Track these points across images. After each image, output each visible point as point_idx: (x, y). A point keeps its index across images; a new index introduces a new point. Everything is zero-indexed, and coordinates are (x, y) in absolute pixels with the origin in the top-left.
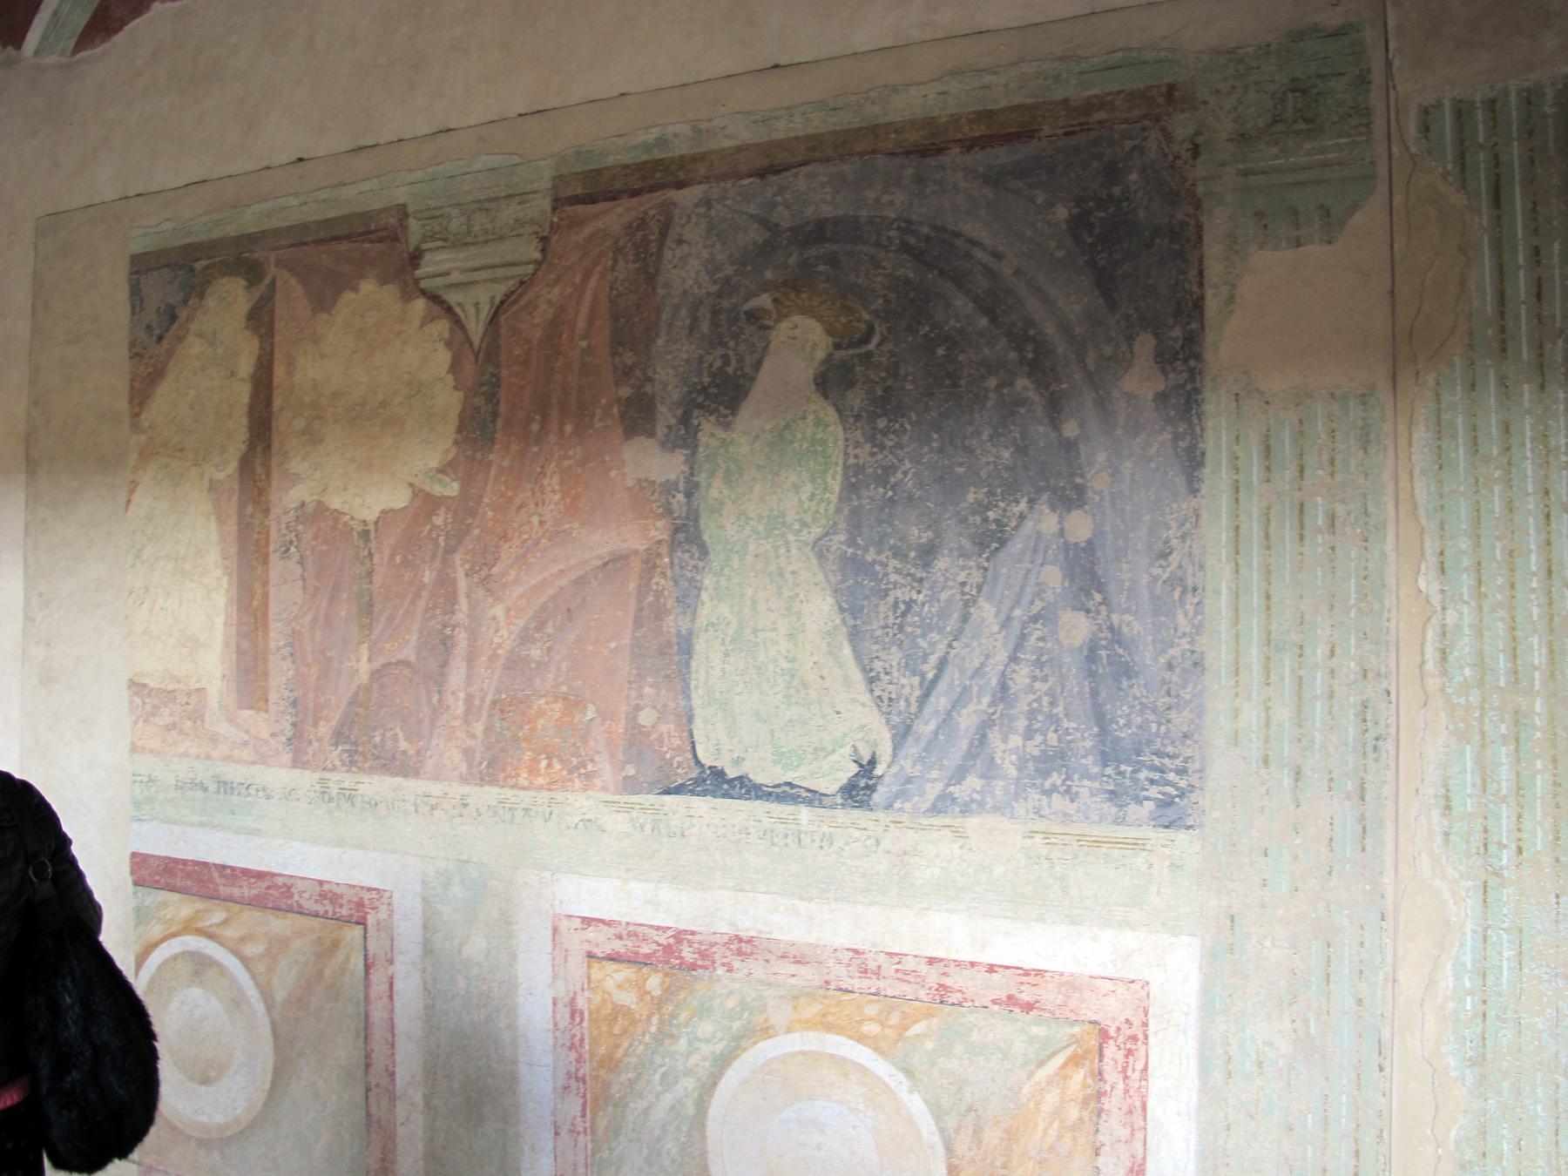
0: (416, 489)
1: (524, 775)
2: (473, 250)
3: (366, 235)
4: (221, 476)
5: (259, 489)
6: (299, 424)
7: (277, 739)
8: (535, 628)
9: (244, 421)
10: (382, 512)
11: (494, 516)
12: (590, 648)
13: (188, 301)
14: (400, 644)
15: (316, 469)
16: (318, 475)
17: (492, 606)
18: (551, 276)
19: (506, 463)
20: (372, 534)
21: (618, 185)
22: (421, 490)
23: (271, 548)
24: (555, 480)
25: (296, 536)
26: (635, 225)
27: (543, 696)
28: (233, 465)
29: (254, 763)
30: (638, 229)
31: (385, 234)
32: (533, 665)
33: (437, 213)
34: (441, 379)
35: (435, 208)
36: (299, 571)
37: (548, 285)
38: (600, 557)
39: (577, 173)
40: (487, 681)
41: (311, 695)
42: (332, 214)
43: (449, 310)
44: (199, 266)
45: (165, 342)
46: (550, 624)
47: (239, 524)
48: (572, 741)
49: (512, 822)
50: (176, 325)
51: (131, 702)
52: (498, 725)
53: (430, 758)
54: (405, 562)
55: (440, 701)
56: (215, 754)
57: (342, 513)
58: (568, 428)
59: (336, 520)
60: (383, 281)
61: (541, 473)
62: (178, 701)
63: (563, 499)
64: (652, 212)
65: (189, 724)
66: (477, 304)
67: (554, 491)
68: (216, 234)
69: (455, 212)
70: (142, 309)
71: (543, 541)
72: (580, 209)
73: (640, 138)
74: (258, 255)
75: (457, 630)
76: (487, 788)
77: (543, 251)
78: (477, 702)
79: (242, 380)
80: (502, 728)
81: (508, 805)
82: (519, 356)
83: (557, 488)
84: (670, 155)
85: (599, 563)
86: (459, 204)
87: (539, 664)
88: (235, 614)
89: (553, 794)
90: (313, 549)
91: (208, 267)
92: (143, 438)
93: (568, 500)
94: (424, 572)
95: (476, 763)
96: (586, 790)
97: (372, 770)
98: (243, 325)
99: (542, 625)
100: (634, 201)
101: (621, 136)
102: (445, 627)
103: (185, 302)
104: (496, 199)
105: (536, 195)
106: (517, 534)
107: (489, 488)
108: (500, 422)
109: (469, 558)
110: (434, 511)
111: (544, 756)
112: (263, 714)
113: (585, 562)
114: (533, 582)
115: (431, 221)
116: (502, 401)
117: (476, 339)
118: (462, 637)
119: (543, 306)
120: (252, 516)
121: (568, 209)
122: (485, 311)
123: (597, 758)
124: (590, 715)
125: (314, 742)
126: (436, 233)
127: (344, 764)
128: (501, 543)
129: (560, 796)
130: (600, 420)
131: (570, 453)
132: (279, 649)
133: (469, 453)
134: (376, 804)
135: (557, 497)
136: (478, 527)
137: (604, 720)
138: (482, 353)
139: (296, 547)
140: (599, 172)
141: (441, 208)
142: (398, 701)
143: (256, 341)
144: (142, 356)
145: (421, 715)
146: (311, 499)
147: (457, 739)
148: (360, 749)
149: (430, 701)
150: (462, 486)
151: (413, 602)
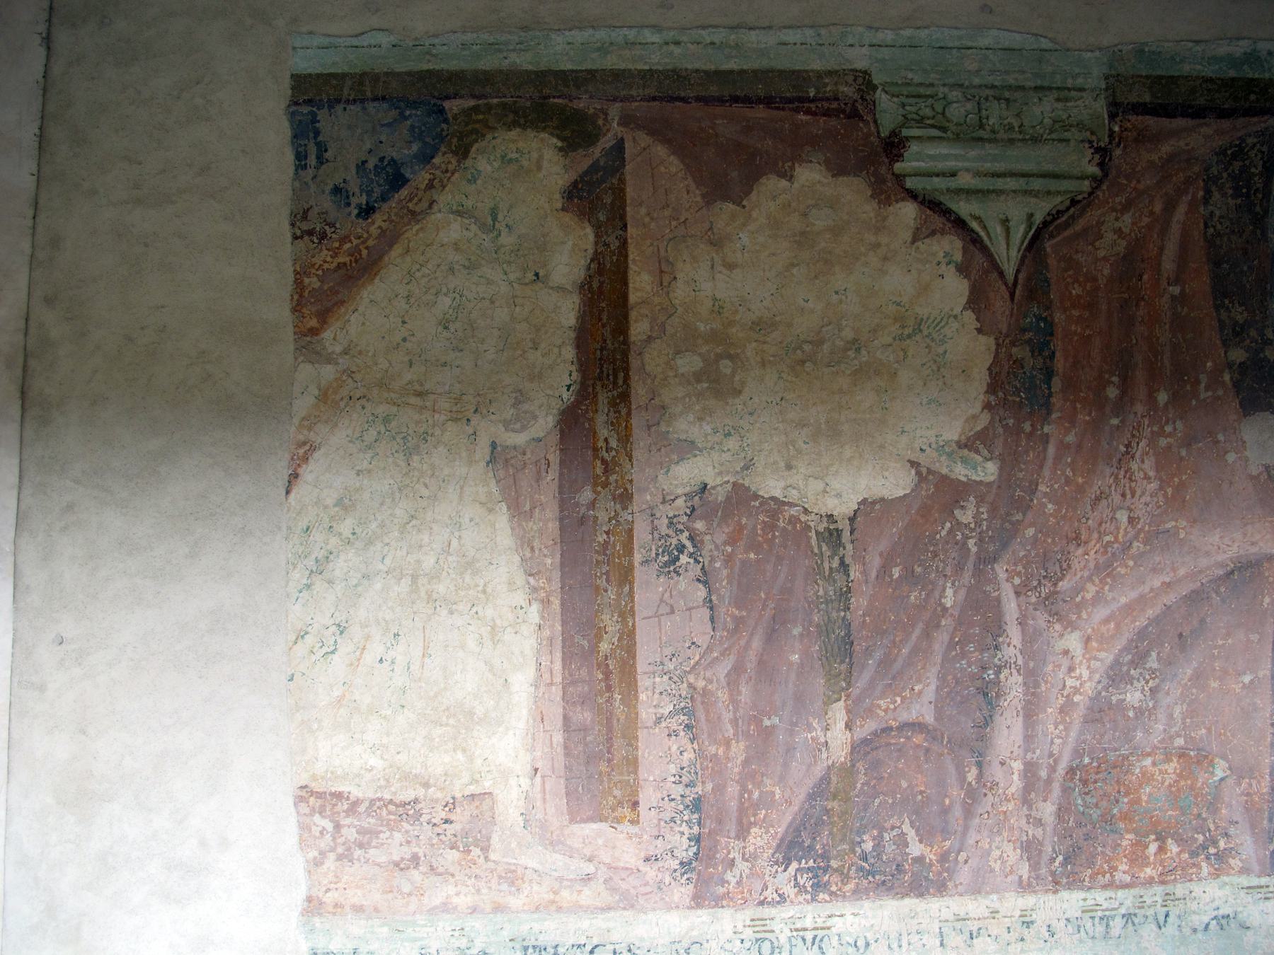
0: (924, 471)
1: (1123, 867)
2: (991, 149)
3: (800, 102)
4: (520, 439)
5: (604, 461)
6: (689, 363)
7: (660, 864)
8: (1132, 662)
9: (569, 353)
10: (865, 500)
11: (1059, 510)
12: (1214, 684)
13: (432, 157)
14: (903, 699)
15: (728, 435)
16: (732, 443)
17: (1061, 636)
18: (1118, 200)
19: (1070, 438)
20: (846, 535)
21: (1201, 101)
22: (929, 471)
23: (638, 558)
24: (1149, 464)
25: (691, 538)
26: (1229, 152)
27: (1149, 755)
28: (545, 423)
29: (609, 908)
30: (1234, 157)
31: (835, 105)
32: (1131, 714)
33: (922, 90)
34: (955, 317)
35: (921, 84)
36: (701, 592)
37: (1113, 209)
38: (1221, 565)
39: (1141, 76)
40: (1057, 741)
41: (733, 789)
42: (732, 65)
43: (960, 224)
44: (453, 106)
45: (379, 220)
46: (1154, 654)
47: (561, 520)
48: (1195, 811)
49: (1106, 936)
50: (404, 192)
51: (304, 828)
52: (1079, 801)
53: (966, 862)
54: (909, 574)
55: (980, 776)
56: (515, 902)
57: (784, 503)
58: (1162, 397)
59: (774, 515)
60: (838, 170)
61: (1127, 453)
62: (424, 818)
63: (1161, 488)
64: (1250, 141)
65: (453, 855)
66: (1005, 222)
67: (1147, 477)
68: (488, 63)
69: (955, 94)
70: (321, 160)
71: (1135, 544)
72: (1150, 121)
73: (1223, 50)
74: (583, 103)
75: (1005, 672)
76: (1064, 894)
77: (1101, 165)
78: (1043, 774)
79: (560, 289)
80: (1085, 805)
81: (1100, 914)
82: (1078, 296)
83: (1152, 474)
84: (1267, 76)
85: (1221, 572)
86: (961, 86)
87: (1139, 712)
88: (558, 666)
89: (1169, 888)
90: (729, 559)
91: (475, 109)
92: (328, 372)
93: (1170, 491)
94: (944, 590)
95: (1045, 858)
96: (1218, 876)
97: (858, 893)
98: (559, 205)
99: (1139, 659)
100: (1226, 124)
101: (1197, 42)
102: (984, 668)
103: (426, 158)
104: (1022, 88)
105: (1084, 94)
106: (1095, 535)
107: (1046, 472)
108: (1057, 383)
109: (1020, 568)
110: (957, 502)
111: (1153, 837)
112: (626, 827)
113: (1200, 572)
114: (1123, 600)
115: (917, 100)
116: (1058, 354)
117: (1010, 270)
118: (1014, 684)
119: (1109, 236)
120: (592, 505)
121: (1133, 118)
122: (1019, 232)
123: (1232, 831)
124: (1219, 774)
125: (738, 860)
126: (923, 118)
127: (801, 889)
128: (1072, 548)
129: (1180, 890)
130: (1207, 388)
131: (1168, 429)
132: (659, 720)
133: (1011, 422)
134: (867, 945)
135: (1154, 486)
136: (1031, 525)
137: (1241, 777)
138: (1019, 287)
139: (691, 555)
140: (1173, 80)
141: (932, 85)
142: (904, 784)
143: (589, 232)
144: (323, 236)
145: (947, 801)
146: (719, 481)
147: (1012, 829)
148: (834, 864)
149: (962, 778)
150: (1001, 469)
151: (927, 635)
